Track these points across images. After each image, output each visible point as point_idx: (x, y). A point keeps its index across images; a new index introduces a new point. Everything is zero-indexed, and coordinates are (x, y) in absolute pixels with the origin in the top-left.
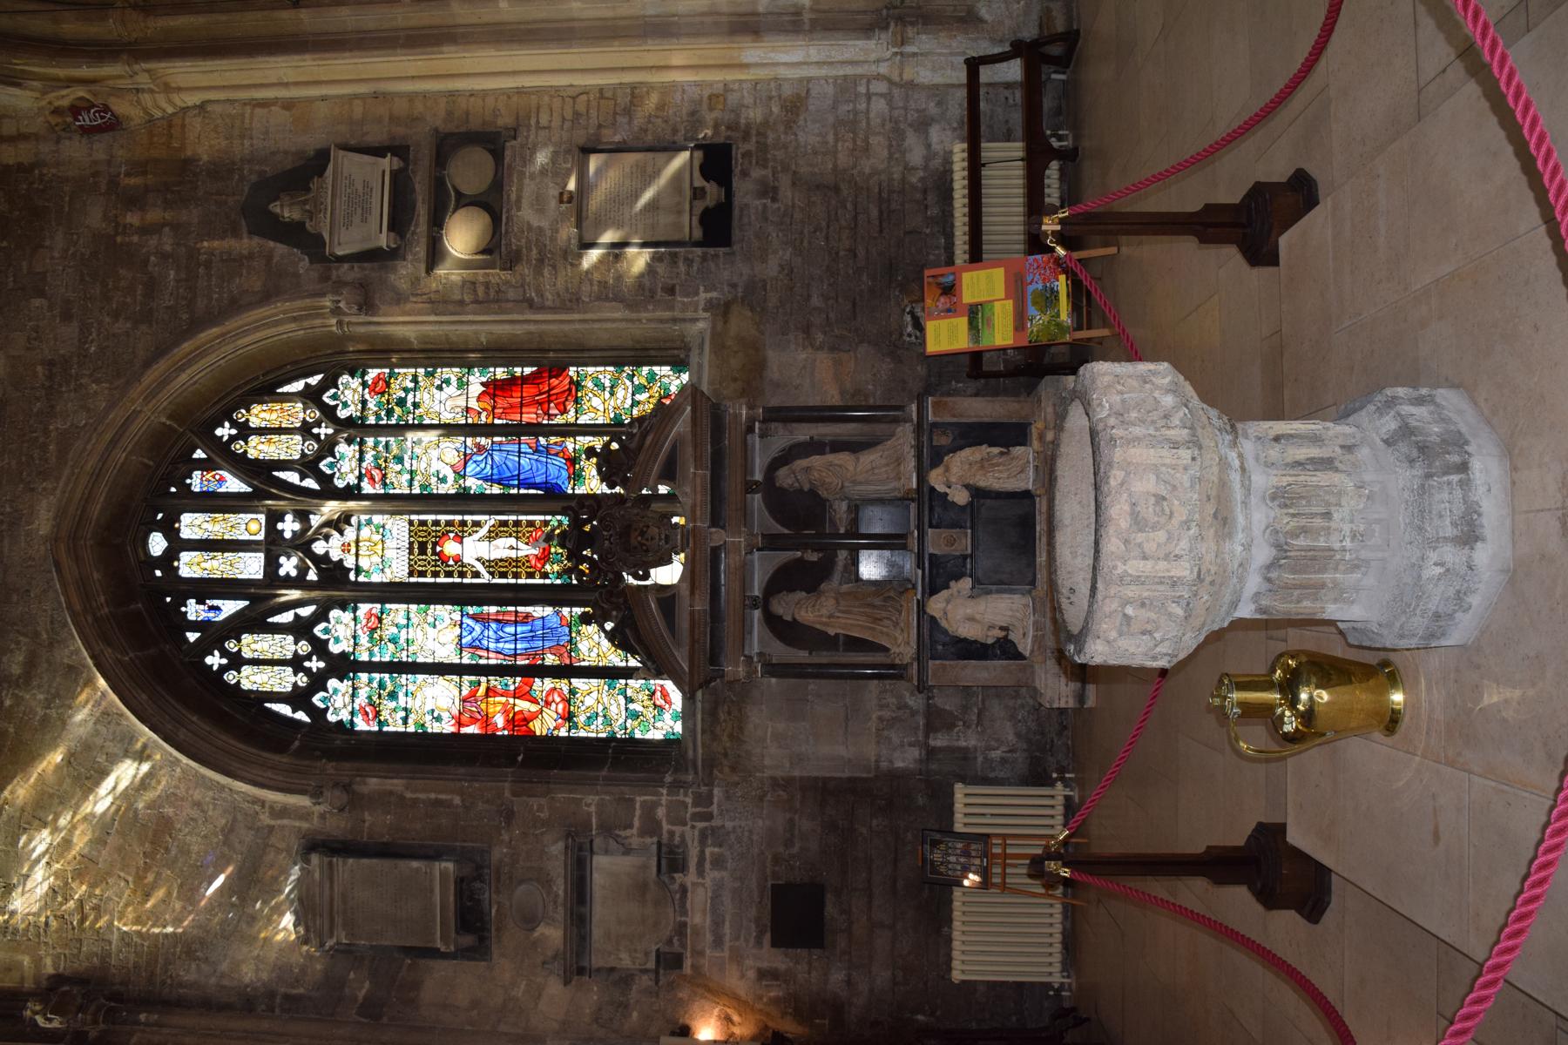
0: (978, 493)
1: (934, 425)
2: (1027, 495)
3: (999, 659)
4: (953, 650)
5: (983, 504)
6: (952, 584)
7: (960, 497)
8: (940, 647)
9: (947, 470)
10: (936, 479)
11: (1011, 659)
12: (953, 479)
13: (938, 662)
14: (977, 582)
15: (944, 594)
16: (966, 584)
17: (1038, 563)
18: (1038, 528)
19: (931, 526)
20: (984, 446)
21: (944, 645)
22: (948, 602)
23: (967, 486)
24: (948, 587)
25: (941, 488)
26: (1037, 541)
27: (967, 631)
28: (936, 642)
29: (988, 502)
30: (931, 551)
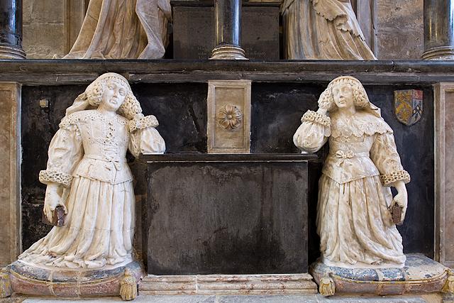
0: (318, 164)
1: (428, 91)
2: (314, 253)
3: (25, 207)
4: (40, 126)
5: (298, 176)
6: (152, 120)
7: (308, 134)
8: (44, 103)
9: (361, 109)
10: (344, 89)
11: (25, 226)
12: (341, 121)
13: (16, 98)
14: (158, 162)
15: (135, 105)
16: (152, 142)
17: (190, 277)
18: (252, 277)
19: (254, 85)
20: (407, 176)
21: (48, 110)
22: (120, 112)
23: (327, 149)
24: (145, 113)
25: (324, 100)
26: (230, 277)
27: (59, 150)
28: (55, 96)
29: (303, 185)
30: (212, 85)
